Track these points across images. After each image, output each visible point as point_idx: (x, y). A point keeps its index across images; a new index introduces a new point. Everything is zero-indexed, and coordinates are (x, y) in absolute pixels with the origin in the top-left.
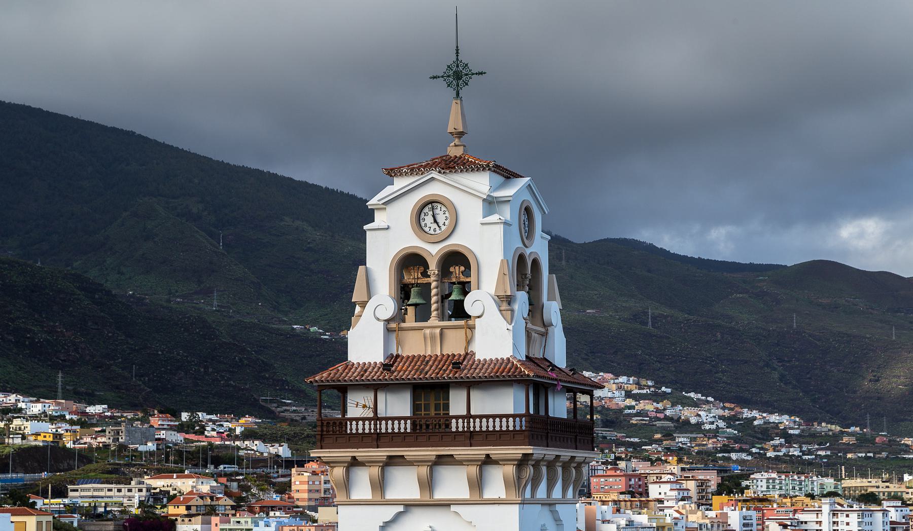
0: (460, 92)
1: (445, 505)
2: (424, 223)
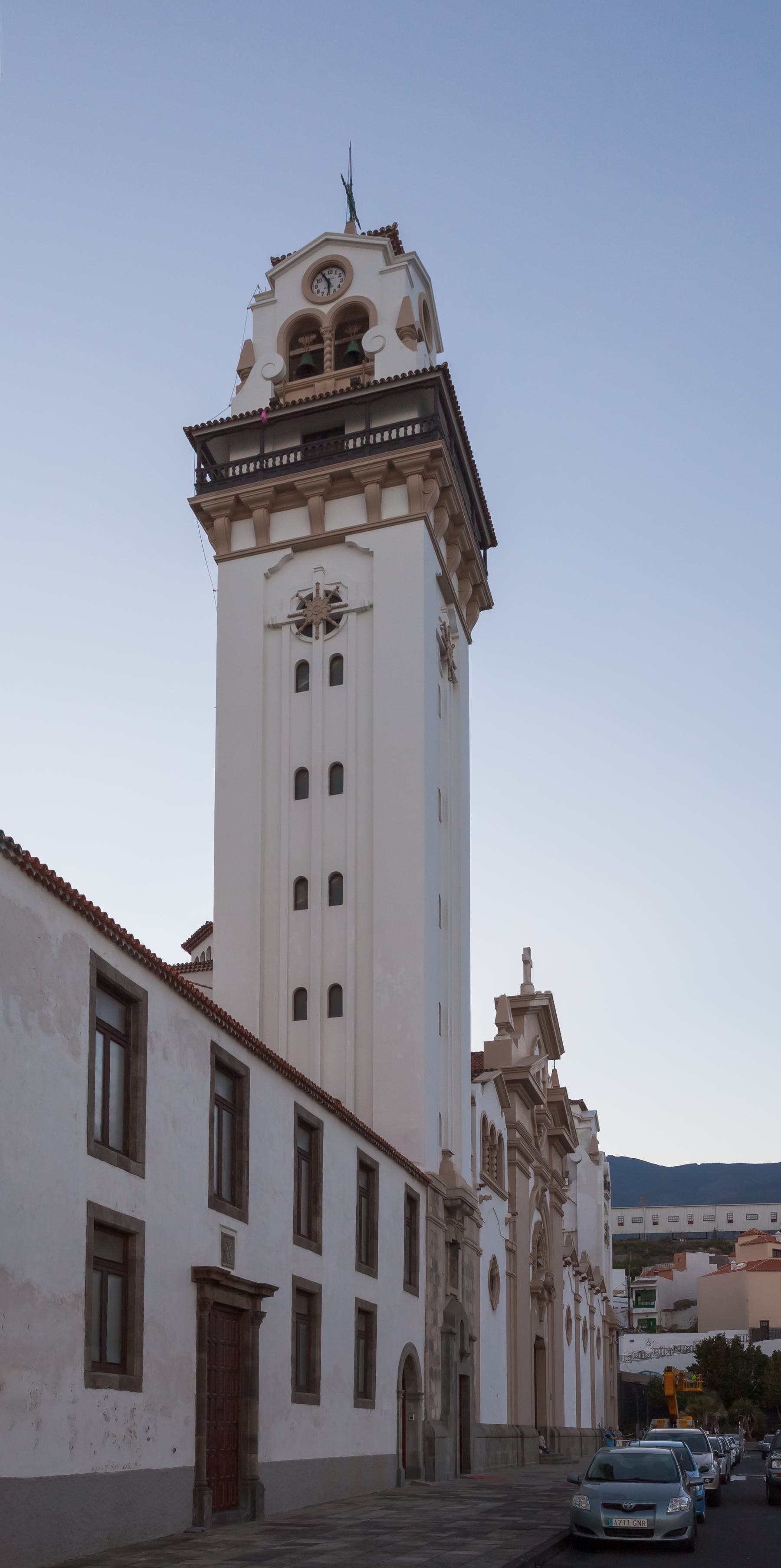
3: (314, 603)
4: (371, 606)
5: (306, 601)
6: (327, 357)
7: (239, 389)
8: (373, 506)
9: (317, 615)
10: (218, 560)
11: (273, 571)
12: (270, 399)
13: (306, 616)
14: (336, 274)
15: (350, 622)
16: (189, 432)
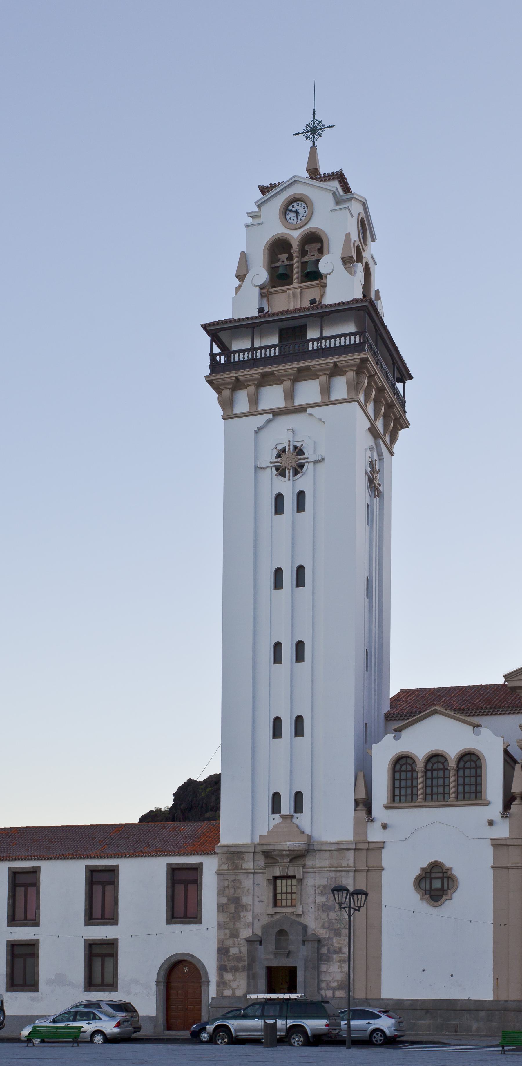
0: (315, 142)
1: (302, 409)
2: (289, 217)
3: (287, 456)
4: (323, 459)
5: (281, 453)
6: (295, 271)
7: (237, 290)
8: (326, 390)
9: (289, 463)
10: (224, 418)
11: (260, 429)
12: (258, 308)
13: (281, 463)
14: (301, 206)
15: (309, 468)
16: (205, 327)
